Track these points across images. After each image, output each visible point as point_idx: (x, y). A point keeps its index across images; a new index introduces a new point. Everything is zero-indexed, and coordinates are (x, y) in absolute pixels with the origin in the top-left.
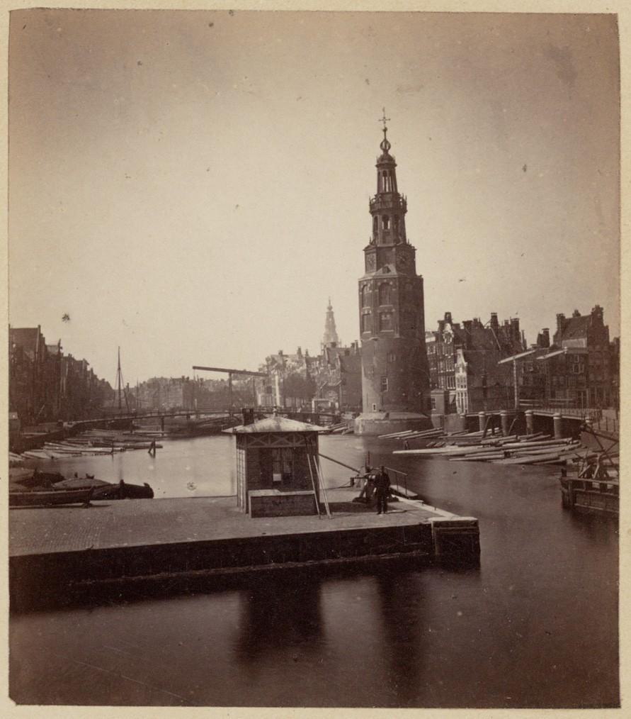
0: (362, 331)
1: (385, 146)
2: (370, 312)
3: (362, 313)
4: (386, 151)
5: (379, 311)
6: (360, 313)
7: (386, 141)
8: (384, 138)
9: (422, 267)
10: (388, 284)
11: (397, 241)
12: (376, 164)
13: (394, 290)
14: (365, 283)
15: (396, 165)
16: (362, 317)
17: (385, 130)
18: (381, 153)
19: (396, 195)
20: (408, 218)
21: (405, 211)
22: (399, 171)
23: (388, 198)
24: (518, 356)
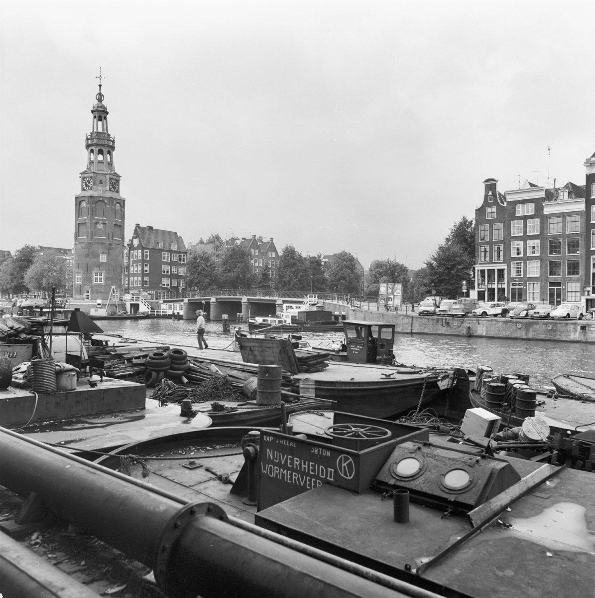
1: (100, 97)
2: (87, 222)
3: (78, 222)
4: (100, 100)
6: (76, 222)
7: (100, 95)
8: (98, 92)
9: (124, 192)
10: (103, 201)
12: (92, 109)
13: (109, 206)
14: (83, 199)
15: (107, 113)
16: (79, 225)
17: (100, 86)
18: (97, 102)
20: (114, 153)
21: (113, 148)
22: (108, 117)
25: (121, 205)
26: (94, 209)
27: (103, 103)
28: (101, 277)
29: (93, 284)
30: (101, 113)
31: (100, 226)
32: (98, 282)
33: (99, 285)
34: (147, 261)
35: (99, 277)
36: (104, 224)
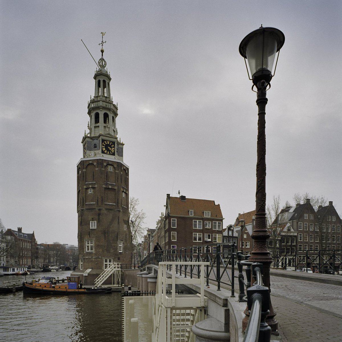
4: (103, 67)
5: (85, 187)
7: (102, 59)
19: (108, 100)
25: (114, 167)
26: (85, 174)
27: (105, 68)
28: (92, 245)
29: (85, 252)
30: (102, 80)
31: (90, 192)
32: (90, 251)
33: (91, 253)
34: (174, 230)
35: (90, 245)
36: (94, 188)
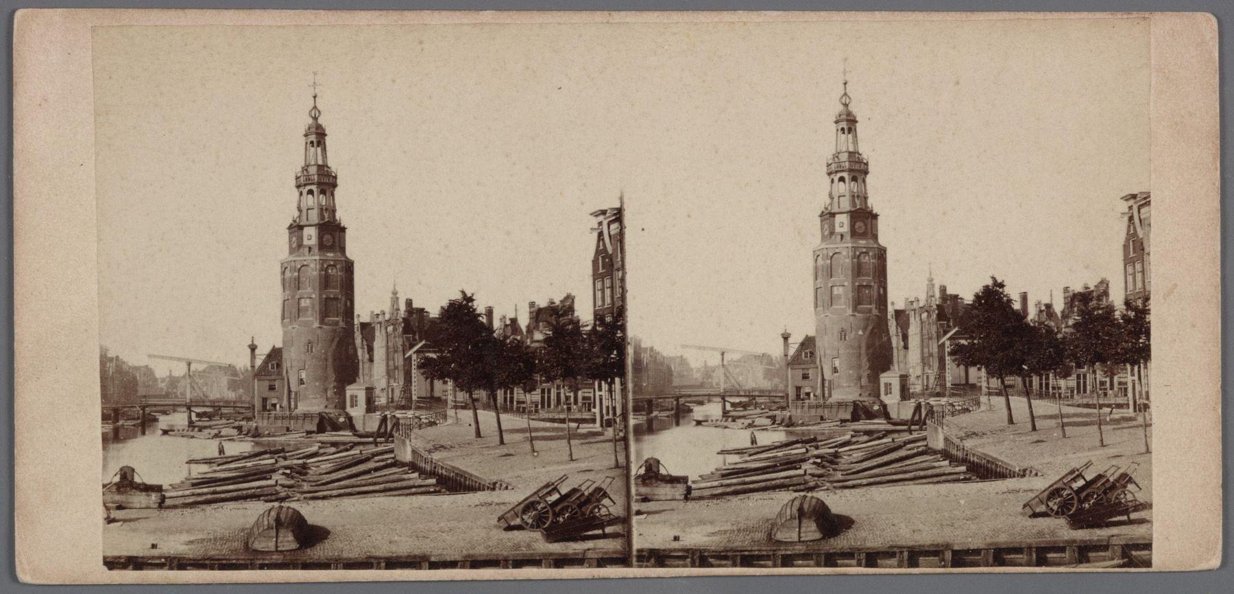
0: (283, 318)
1: (315, 114)
4: (315, 119)
11: (322, 216)
18: (310, 121)
20: (337, 192)
21: (335, 185)
23: (313, 170)
24: (415, 348)
